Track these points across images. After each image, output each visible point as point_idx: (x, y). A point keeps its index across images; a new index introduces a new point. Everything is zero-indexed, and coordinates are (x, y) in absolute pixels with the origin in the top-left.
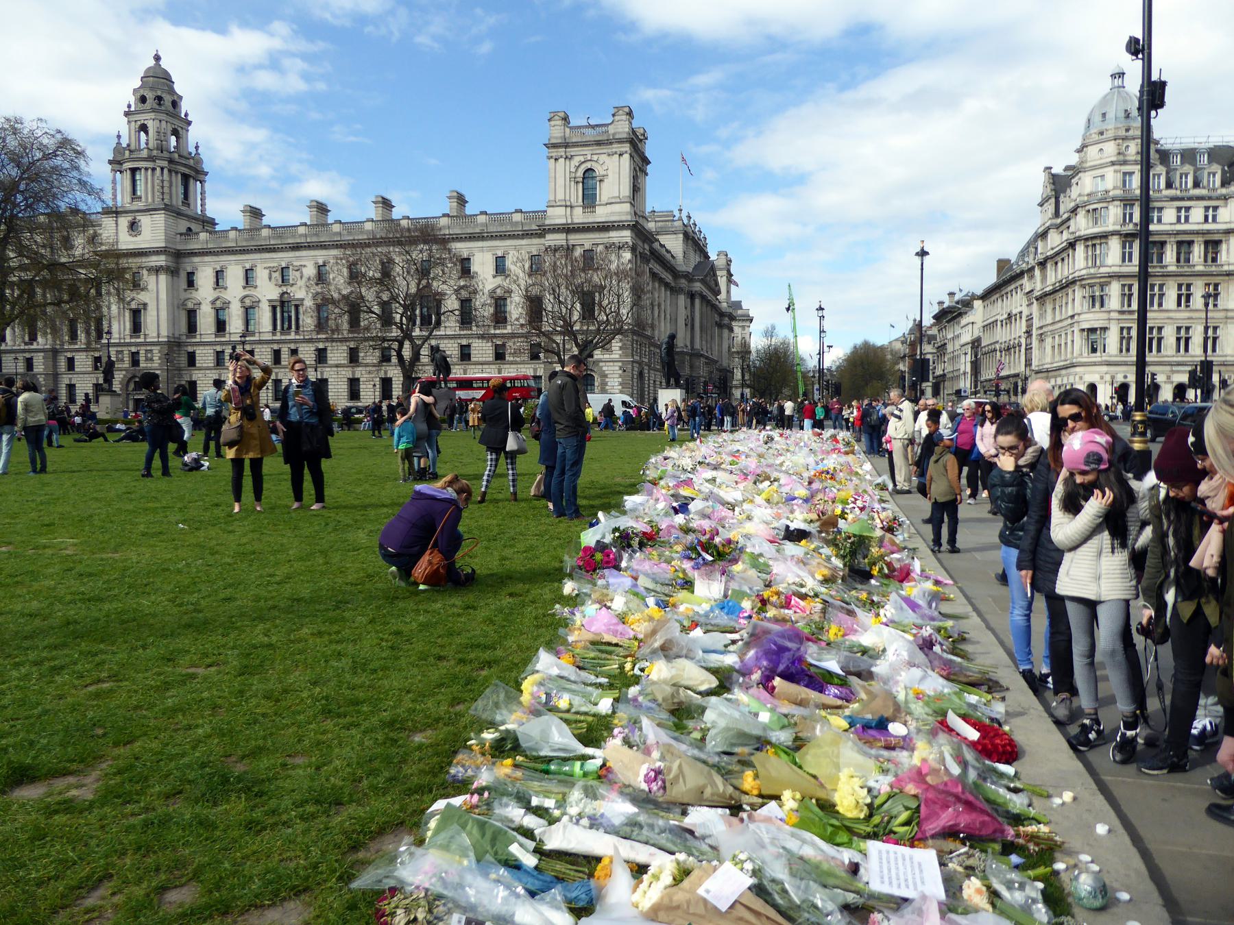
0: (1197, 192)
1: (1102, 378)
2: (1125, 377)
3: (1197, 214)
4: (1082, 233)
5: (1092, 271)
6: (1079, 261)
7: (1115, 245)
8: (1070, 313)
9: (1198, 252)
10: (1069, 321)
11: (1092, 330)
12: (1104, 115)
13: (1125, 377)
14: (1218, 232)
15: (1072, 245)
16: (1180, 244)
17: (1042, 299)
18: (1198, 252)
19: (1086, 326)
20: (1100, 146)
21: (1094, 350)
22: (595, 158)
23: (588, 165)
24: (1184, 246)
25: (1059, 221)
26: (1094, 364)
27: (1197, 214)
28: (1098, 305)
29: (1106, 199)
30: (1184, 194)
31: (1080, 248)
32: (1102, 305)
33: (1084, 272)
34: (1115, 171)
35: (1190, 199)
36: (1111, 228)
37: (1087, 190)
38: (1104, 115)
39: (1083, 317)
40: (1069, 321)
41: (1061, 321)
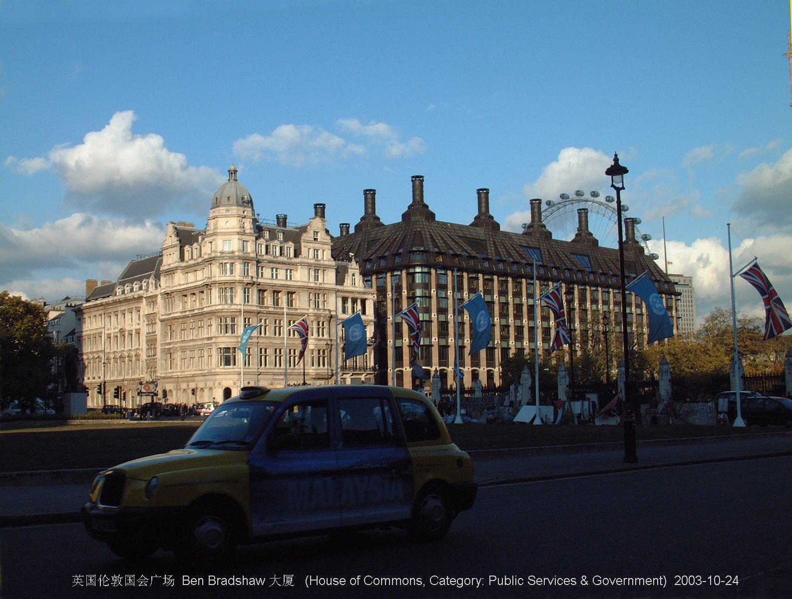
1: (235, 384)
2: (249, 383)
4: (217, 279)
5: (226, 307)
6: (215, 298)
7: (239, 291)
9: (283, 298)
10: (206, 342)
11: (227, 349)
12: (229, 198)
13: (249, 383)
14: (294, 287)
16: (276, 292)
17: (168, 323)
18: (283, 298)
19: (223, 346)
20: (227, 219)
21: (227, 362)
25: (184, 264)
26: (230, 373)
27: (282, 274)
28: (230, 331)
29: (232, 256)
30: (275, 259)
31: (215, 292)
32: (233, 332)
34: (239, 239)
35: (279, 263)
36: (237, 278)
37: (220, 249)
38: (229, 198)
39: (219, 340)
40: (206, 342)
41: (193, 340)
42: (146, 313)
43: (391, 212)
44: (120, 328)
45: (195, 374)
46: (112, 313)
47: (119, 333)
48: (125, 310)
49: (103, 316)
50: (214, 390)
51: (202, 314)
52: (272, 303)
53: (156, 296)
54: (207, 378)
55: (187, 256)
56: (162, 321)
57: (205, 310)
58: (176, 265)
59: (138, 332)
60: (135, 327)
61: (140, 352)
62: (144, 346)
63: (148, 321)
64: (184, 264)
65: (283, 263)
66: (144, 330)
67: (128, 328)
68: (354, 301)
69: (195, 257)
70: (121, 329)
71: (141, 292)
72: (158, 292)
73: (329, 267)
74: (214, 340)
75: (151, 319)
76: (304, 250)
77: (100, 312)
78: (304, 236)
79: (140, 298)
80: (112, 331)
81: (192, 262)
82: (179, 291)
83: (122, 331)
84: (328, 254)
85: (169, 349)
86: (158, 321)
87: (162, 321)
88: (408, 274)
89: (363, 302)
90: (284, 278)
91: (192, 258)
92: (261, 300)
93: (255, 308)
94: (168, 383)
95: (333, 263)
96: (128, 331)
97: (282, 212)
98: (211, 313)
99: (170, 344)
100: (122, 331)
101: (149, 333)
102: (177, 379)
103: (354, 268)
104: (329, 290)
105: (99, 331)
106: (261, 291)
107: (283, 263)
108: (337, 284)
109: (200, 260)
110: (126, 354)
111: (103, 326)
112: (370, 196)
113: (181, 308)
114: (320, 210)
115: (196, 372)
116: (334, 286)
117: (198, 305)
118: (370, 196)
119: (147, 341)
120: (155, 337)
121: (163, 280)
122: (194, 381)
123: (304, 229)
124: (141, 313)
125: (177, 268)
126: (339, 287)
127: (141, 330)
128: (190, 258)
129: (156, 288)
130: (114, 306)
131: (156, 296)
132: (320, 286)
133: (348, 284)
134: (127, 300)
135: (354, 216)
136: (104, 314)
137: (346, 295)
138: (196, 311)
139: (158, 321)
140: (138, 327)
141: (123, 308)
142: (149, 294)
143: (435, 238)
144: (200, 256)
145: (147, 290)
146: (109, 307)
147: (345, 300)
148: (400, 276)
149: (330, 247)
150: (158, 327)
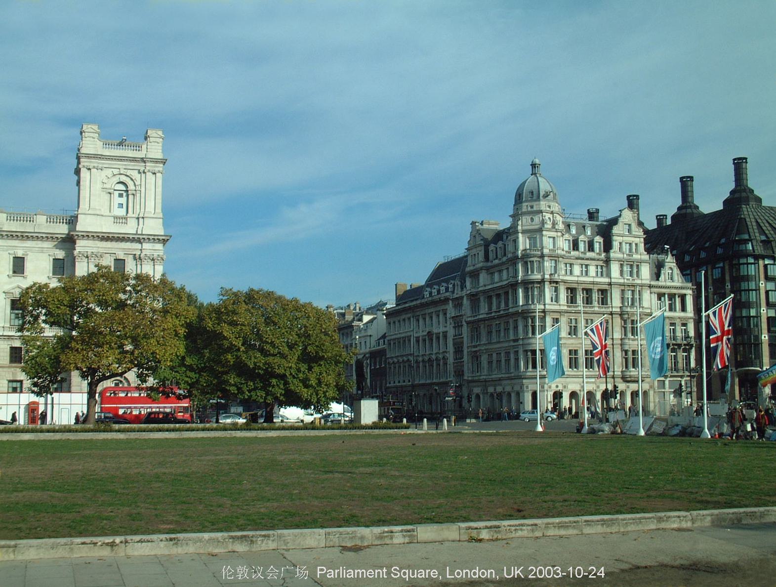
0: (590, 255)
2: (557, 386)
3: (592, 270)
8: (512, 337)
9: (595, 296)
10: (512, 344)
13: (557, 386)
15: (514, 286)
17: (475, 325)
22: (129, 173)
23: (123, 178)
24: (588, 291)
25: (489, 264)
27: (592, 270)
33: (525, 308)
35: (587, 259)
38: (532, 193)
40: (512, 344)
42: (453, 315)
43: (710, 202)
44: (427, 330)
45: (502, 377)
47: (427, 337)
48: (432, 312)
49: (412, 319)
50: (521, 395)
51: (507, 315)
52: (566, 301)
53: (462, 298)
54: (513, 381)
55: (491, 256)
56: (468, 323)
57: (511, 310)
58: (481, 265)
59: (445, 335)
61: (448, 355)
62: (451, 348)
64: (489, 264)
65: (594, 259)
66: (451, 333)
67: (435, 331)
68: (672, 297)
69: (499, 256)
70: (429, 332)
71: (447, 294)
72: (464, 293)
73: (645, 262)
74: (521, 342)
75: (457, 322)
76: (616, 245)
77: (409, 315)
78: (616, 230)
79: (446, 300)
80: (421, 334)
81: (497, 262)
82: (484, 292)
83: (430, 334)
84: (642, 247)
85: (476, 352)
86: (464, 323)
87: (468, 323)
88: (731, 266)
89: (683, 297)
90: (594, 275)
91: (497, 257)
92: (572, 300)
93: (565, 308)
94: (475, 387)
95: (646, 257)
96: (436, 334)
97: (593, 207)
98: (517, 314)
99: (475, 346)
100: (430, 334)
101: (456, 336)
102: (484, 383)
103: (670, 261)
104: (642, 286)
105: (409, 334)
106: (572, 291)
107: (594, 259)
108: (652, 279)
109: (504, 259)
110: (434, 357)
111: (412, 329)
112: (686, 183)
113: (487, 309)
114: (632, 202)
115: (503, 376)
116: (648, 282)
117: (503, 305)
118: (686, 183)
119: (454, 344)
120: (461, 340)
122: (501, 385)
123: (614, 222)
124: (448, 316)
125: (481, 269)
126: (654, 283)
127: (448, 333)
128: (495, 257)
129: (462, 289)
131: (462, 298)
132: (633, 282)
133: (664, 280)
135: (670, 207)
137: (663, 291)
138: (502, 312)
139: (464, 323)
140: (445, 330)
141: (430, 311)
142: (455, 296)
143: (762, 225)
144: (505, 255)
145: (453, 292)
147: (660, 296)
148: (723, 268)
149: (642, 240)
150: (465, 330)
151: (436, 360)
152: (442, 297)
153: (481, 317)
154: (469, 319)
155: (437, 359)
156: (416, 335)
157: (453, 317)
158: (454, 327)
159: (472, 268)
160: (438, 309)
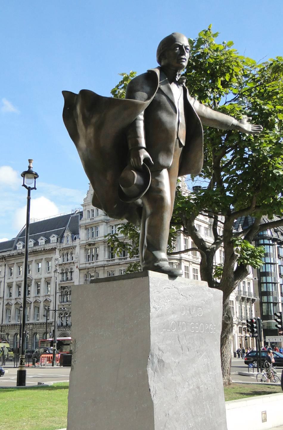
46: (15, 264)
53: (74, 247)
60: (43, 275)
63: (62, 270)
72: (77, 242)
113: (107, 257)
121: (82, 233)
125: (103, 221)
130: (18, 258)
134: (45, 251)
136: (5, 265)
140: (48, 275)
142: (64, 245)
146: (11, 259)
151: (34, 302)
152: (48, 247)
153: (99, 263)
154: (82, 266)
155: (36, 302)
156: (7, 281)
157: (60, 265)
158: (62, 273)
159: (88, 221)
160: (39, 257)
